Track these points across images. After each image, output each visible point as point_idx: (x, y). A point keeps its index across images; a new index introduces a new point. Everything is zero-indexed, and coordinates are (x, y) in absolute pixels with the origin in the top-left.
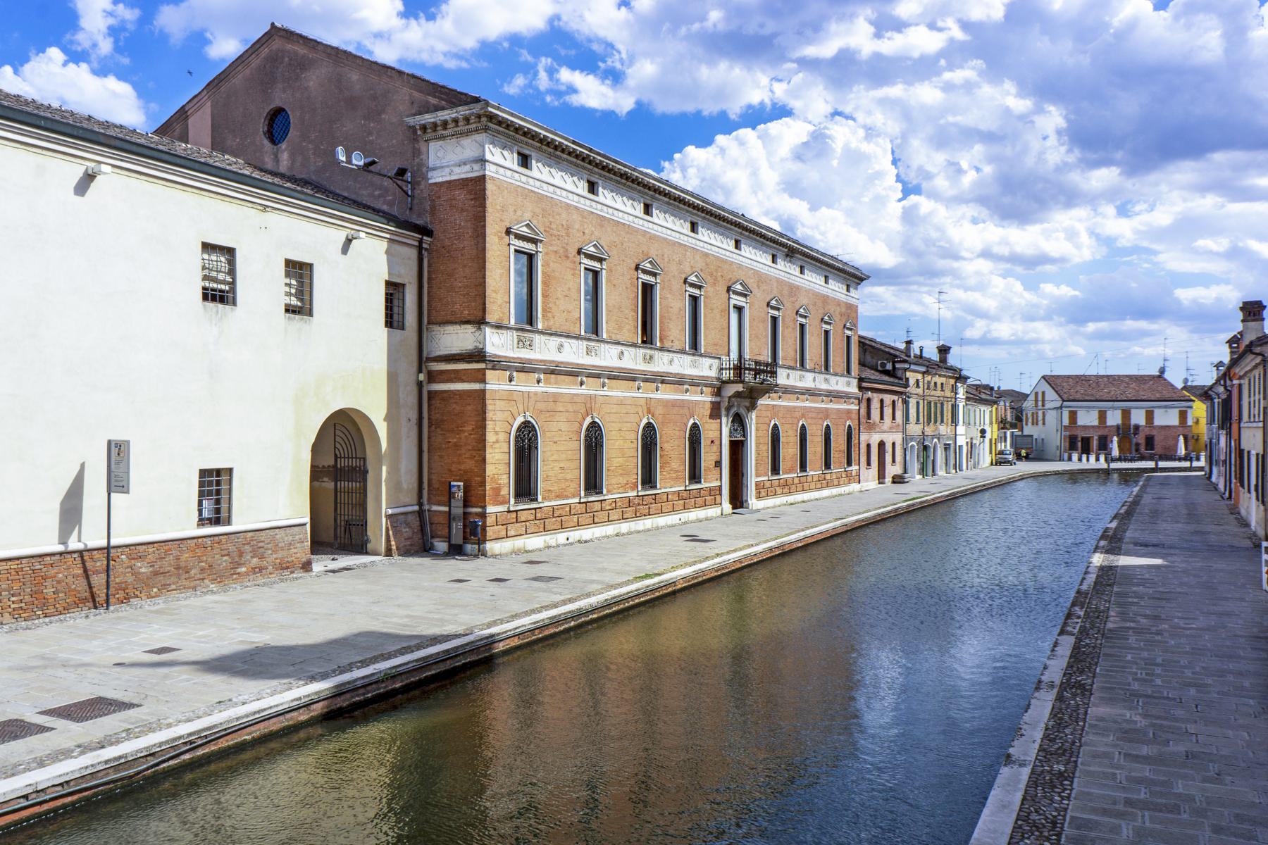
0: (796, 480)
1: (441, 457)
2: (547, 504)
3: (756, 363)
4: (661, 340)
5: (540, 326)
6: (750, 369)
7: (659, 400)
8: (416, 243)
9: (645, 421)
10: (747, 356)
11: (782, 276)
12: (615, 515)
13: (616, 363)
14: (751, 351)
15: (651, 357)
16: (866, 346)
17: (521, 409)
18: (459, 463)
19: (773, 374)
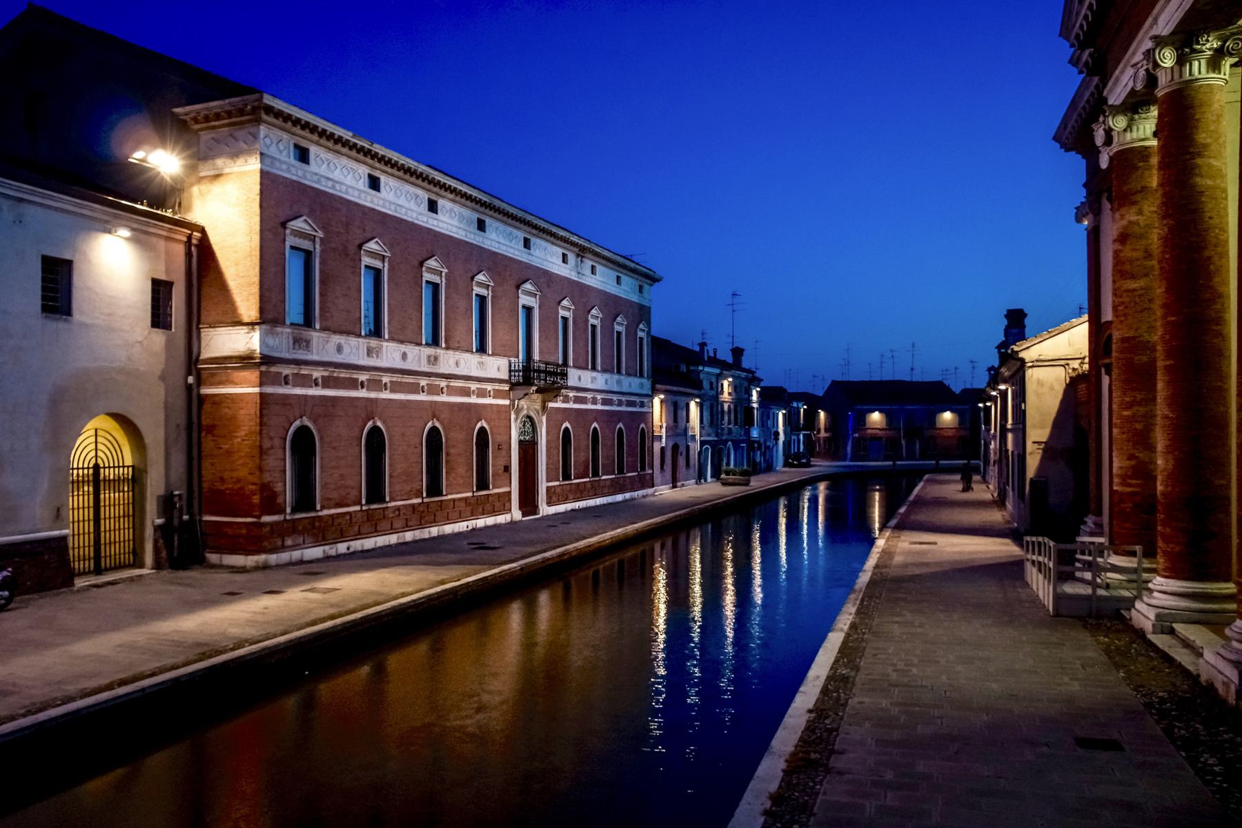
0: (589, 485)
1: (212, 464)
2: (326, 512)
3: (547, 364)
4: (446, 342)
5: (318, 327)
6: (539, 371)
7: (444, 403)
8: (185, 239)
9: (429, 425)
10: (536, 357)
11: (573, 276)
12: (398, 524)
13: (399, 364)
14: (541, 352)
15: (436, 358)
16: (661, 346)
17: (297, 414)
18: (232, 470)
19: (564, 375)
